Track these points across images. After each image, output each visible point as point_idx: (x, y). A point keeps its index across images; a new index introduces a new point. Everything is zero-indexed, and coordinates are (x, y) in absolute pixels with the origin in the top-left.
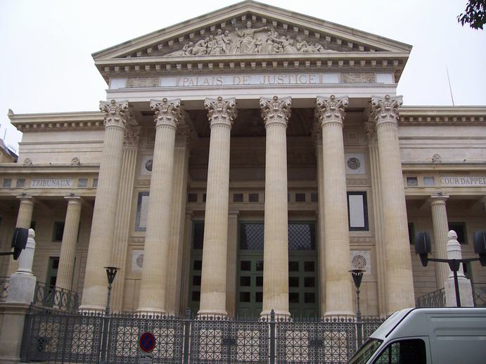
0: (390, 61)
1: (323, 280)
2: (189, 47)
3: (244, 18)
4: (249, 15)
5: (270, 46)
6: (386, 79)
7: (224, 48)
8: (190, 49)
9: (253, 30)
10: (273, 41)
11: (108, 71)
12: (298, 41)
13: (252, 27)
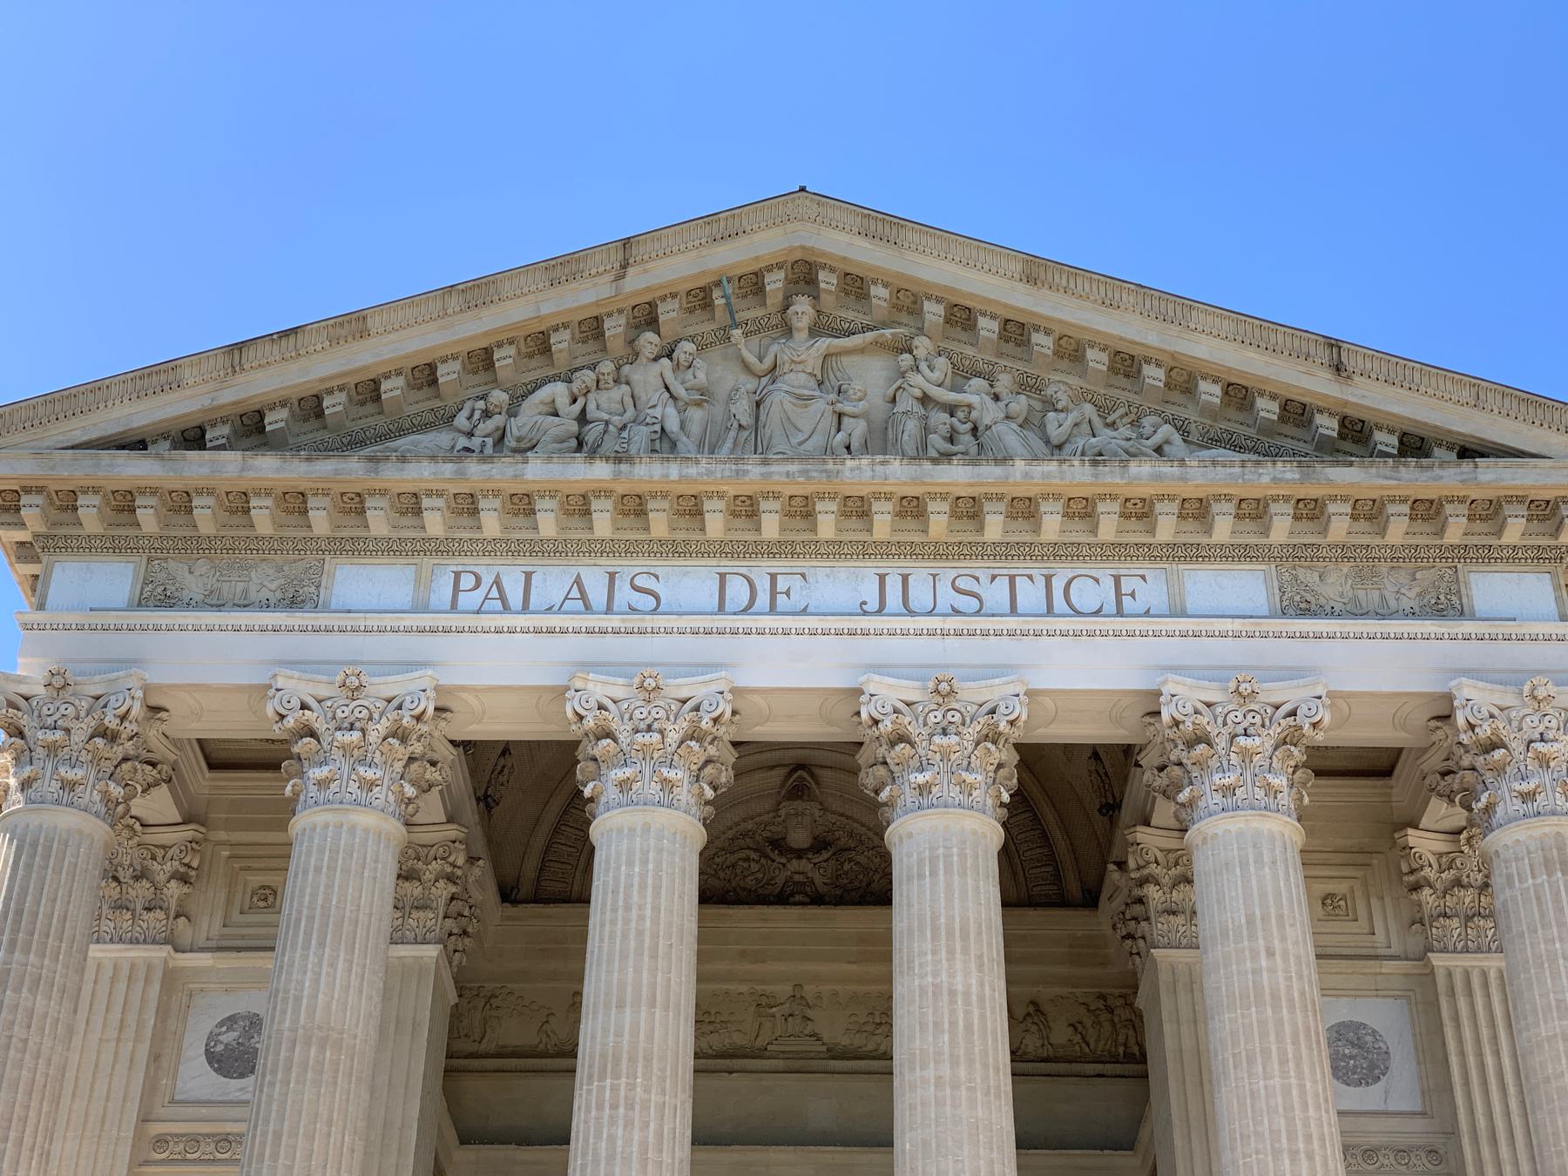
2: (487, 414)
3: (775, 283)
4: (804, 274)
5: (912, 427)
7: (673, 425)
9: (824, 343)
10: (925, 400)
12: (1050, 405)
13: (815, 331)
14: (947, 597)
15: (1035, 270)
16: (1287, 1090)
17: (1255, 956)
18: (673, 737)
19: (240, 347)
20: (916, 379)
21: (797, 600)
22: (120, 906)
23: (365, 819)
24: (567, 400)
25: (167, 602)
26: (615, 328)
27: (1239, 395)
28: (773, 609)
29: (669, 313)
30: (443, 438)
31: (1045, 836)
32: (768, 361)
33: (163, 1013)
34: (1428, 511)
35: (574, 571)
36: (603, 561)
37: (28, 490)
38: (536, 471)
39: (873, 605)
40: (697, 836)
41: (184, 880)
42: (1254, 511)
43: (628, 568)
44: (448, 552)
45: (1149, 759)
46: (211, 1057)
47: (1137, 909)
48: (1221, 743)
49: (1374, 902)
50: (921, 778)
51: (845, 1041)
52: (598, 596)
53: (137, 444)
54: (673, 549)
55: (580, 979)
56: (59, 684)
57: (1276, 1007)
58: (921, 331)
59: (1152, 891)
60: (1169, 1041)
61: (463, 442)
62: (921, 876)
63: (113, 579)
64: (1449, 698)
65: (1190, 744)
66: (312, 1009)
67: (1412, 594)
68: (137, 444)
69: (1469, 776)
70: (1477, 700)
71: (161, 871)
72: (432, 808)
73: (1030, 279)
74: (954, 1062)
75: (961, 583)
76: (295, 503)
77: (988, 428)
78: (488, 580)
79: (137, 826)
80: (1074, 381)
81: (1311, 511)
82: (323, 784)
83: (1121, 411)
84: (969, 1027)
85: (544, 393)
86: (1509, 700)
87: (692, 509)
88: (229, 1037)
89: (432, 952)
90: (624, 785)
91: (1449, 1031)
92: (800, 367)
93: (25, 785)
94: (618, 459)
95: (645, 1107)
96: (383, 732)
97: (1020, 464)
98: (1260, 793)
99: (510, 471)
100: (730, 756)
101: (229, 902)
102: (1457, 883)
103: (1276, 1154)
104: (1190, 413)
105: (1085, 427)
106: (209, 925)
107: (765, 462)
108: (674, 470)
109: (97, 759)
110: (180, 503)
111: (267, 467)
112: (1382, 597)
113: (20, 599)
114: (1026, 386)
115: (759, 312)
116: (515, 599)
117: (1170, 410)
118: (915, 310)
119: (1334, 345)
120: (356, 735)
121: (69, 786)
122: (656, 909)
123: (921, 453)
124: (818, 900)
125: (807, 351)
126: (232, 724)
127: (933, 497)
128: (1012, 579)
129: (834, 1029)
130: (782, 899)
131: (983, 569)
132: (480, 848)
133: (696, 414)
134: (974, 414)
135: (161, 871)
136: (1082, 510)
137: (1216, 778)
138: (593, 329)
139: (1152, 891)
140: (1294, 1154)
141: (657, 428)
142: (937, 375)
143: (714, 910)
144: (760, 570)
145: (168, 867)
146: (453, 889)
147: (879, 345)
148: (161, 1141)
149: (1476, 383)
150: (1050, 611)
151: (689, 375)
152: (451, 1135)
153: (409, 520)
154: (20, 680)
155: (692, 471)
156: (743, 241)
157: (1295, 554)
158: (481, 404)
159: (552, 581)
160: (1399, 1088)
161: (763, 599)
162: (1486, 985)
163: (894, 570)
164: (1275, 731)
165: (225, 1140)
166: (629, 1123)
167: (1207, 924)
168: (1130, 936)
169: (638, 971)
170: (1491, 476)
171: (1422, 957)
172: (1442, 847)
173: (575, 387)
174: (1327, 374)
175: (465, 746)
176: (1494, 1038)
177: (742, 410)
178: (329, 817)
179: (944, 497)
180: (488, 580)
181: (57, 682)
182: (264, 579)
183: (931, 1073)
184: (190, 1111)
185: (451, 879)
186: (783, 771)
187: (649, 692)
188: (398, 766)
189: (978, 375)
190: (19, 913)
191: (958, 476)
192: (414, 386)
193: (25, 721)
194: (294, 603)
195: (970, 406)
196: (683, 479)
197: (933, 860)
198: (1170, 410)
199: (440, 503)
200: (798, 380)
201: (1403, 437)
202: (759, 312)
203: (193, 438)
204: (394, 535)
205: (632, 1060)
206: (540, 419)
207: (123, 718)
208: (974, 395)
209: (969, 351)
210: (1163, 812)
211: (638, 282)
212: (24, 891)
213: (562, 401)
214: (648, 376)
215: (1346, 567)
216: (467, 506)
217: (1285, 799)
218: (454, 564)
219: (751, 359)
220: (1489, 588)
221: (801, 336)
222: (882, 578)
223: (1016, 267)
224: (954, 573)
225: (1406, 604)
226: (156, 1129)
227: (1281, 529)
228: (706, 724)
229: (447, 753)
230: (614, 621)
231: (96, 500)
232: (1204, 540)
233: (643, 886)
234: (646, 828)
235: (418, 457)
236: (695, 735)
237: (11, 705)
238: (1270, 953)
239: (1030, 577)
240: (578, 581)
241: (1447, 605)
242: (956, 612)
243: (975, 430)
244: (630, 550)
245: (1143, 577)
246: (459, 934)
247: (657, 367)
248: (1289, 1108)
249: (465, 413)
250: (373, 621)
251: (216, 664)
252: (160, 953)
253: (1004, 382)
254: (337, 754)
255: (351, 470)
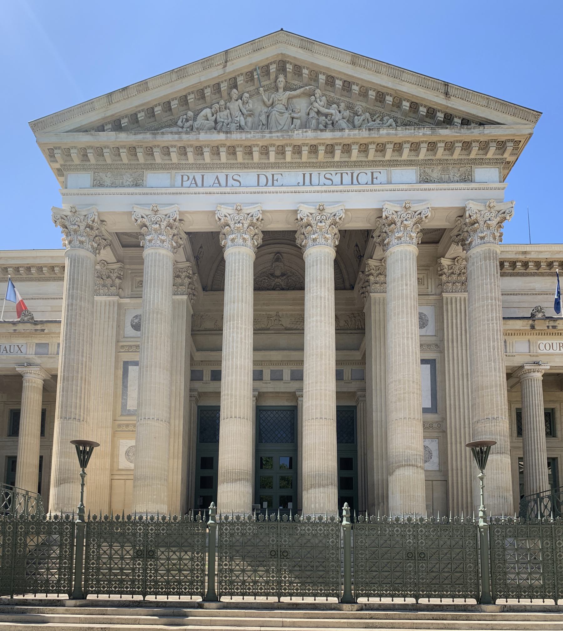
0: (502, 145)
1: (377, 476)
2: (187, 120)
5: (314, 121)
6: (486, 174)
7: (243, 123)
8: (188, 124)
9: (288, 93)
10: (318, 113)
11: (62, 160)
12: (356, 114)
14: (323, 180)
15: (356, 59)
16: (407, 322)
17: (402, 286)
18: (246, 225)
19: (111, 94)
20: (316, 105)
21: (280, 182)
22: (104, 286)
23: (163, 252)
24: (211, 115)
25: (101, 185)
26: (224, 87)
27: (414, 106)
28: (273, 185)
29: (240, 81)
30: (175, 129)
31: (341, 271)
32: (271, 100)
33: (119, 315)
34: (467, 146)
35: (216, 174)
36: (224, 171)
37: (56, 148)
38: (203, 137)
39: (302, 183)
40: (253, 256)
41: (120, 278)
42: (415, 147)
43: (232, 173)
44: (180, 169)
45: (375, 234)
46: (133, 326)
47: (367, 284)
48: (399, 224)
49: (429, 280)
50: (314, 237)
51: (289, 326)
52: (223, 182)
53: (85, 130)
54: (244, 166)
55: (222, 311)
56: (74, 212)
57: (407, 300)
58: (318, 87)
59: (371, 278)
60: (374, 317)
61: (180, 130)
62: (313, 266)
63: (85, 178)
64: (464, 209)
65: (389, 225)
66: (154, 304)
67: (458, 176)
68: (85, 130)
69: (466, 234)
70: (473, 208)
71: (113, 276)
72: (181, 257)
73: (353, 63)
74: (321, 316)
75: (327, 176)
76: (132, 150)
77: (337, 122)
78: (191, 178)
79: (105, 263)
80: (364, 104)
81: (432, 146)
82: (150, 241)
83: (377, 115)
84: (325, 307)
85: (203, 113)
86: (482, 208)
87: (249, 152)
88: (136, 321)
89: (185, 297)
90: (233, 240)
91: (445, 314)
92: (280, 102)
93: (70, 242)
94: (227, 133)
95: (241, 328)
96: (165, 225)
97: (347, 131)
98: (408, 239)
99: (195, 137)
100: (261, 236)
101: (132, 285)
102: (453, 273)
103: (403, 338)
104: (399, 115)
105: (366, 121)
106: (128, 292)
107: (271, 132)
108: (244, 136)
109: (88, 235)
110: (100, 152)
111: (123, 137)
112: (449, 177)
113: (59, 186)
114: (350, 107)
115: (268, 82)
116: (199, 183)
117: (393, 114)
118: (316, 80)
119: (446, 84)
120: (158, 225)
121: (82, 242)
122: (242, 276)
123: (317, 129)
124: (283, 289)
125: (283, 96)
126: (125, 226)
127: (320, 144)
128: (342, 174)
129: (286, 323)
130: (274, 289)
131: (333, 171)
132: (196, 271)
133: (249, 119)
134: (333, 117)
135: (113, 276)
136: (364, 148)
137: (397, 235)
138: (217, 88)
139: (371, 278)
140: (408, 338)
141: (238, 124)
142: (322, 103)
143: (256, 292)
144: (269, 173)
145: (115, 275)
146: (190, 280)
147: (304, 93)
148: (123, 347)
149: (488, 98)
150: (352, 183)
151: (247, 106)
152: (195, 350)
153: (166, 157)
154: (63, 210)
155: (249, 136)
156: (263, 51)
157: (427, 163)
158: (185, 116)
159: (210, 177)
160: (430, 329)
161: (270, 182)
162: (456, 301)
163: (307, 171)
164: (414, 220)
165: (137, 347)
166: (237, 333)
167: (388, 279)
168: (363, 293)
169: (238, 293)
170: (490, 132)
171: (440, 294)
172: (449, 263)
173: (213, 110)
174: (443, 96)
175: (188, 234)
176: (457, 315)
177: (263, 118)
178: (153, 251)
179: (323, 144)
180: (191, 178)
181: (73, 210)
182: (128, 178)
183: (315, 318)
184: (129, 339)
185: (189, 277)
186: (274, 254)
187: (239, 211)
188: (171, 237)
189: (335, 103)
190: (74, 279)
191: (328, 136)
192: (164, 111)
193: (67, 223)
194: (137, 185)
195: (332, 115)
196: (247, 139)
197: (317, 261)
198: (393, 114)
199: (175, 149)
200: (280, 107)
201: (463, 119)
202: (268, 82)
203: (101, 129)
204: (163, 163)
205: (238, 316)
206: (203, 121)
207: (93, 221)
208: (333, 110)
209: (332, 95)
210: (378, 254)
211: (230, 68)
212: (74, 272)
213: (209, 115)
214: (235, 106)
215: (440, 167)
216: (183, 151)
217: (415, 241)
218: (182, 172)
219: (266, 100)
220: (480, 173)
221: (281, 90)
222: (304, 175)
223: (349, 59)
224: (325, 173)
225: (456, 179)
226: (121, 344)
227: (423, 154)
228: (255, 221)
229: (184, 236)
230: (228, 190)
231: (75, 151)
232: (399, 159)
233: (239, 269)
234: (239, 253)
235: (167, 133)
236: (252, 224)
237: (62, 218)
238: (406, 285)
239: (347, 173)
240: (217, 177)
241: (467, 179)
242: (325, 184)
243: (333, 123)
244: (231, 166)
245: (380, 172)
246: (192, 295)
247: (237, 103)
248: (408, 326)
249: (180, 120)
250: (159, 190)
251: (118, 205)
252: (116, 298)
253: (343, 105)
254: (153, 232)
255: (147, 138)
